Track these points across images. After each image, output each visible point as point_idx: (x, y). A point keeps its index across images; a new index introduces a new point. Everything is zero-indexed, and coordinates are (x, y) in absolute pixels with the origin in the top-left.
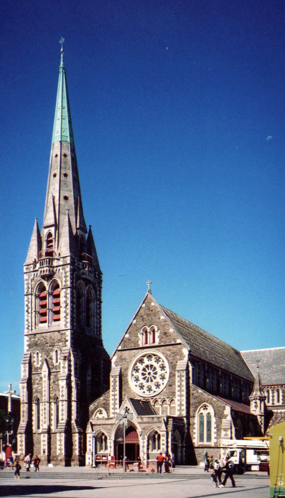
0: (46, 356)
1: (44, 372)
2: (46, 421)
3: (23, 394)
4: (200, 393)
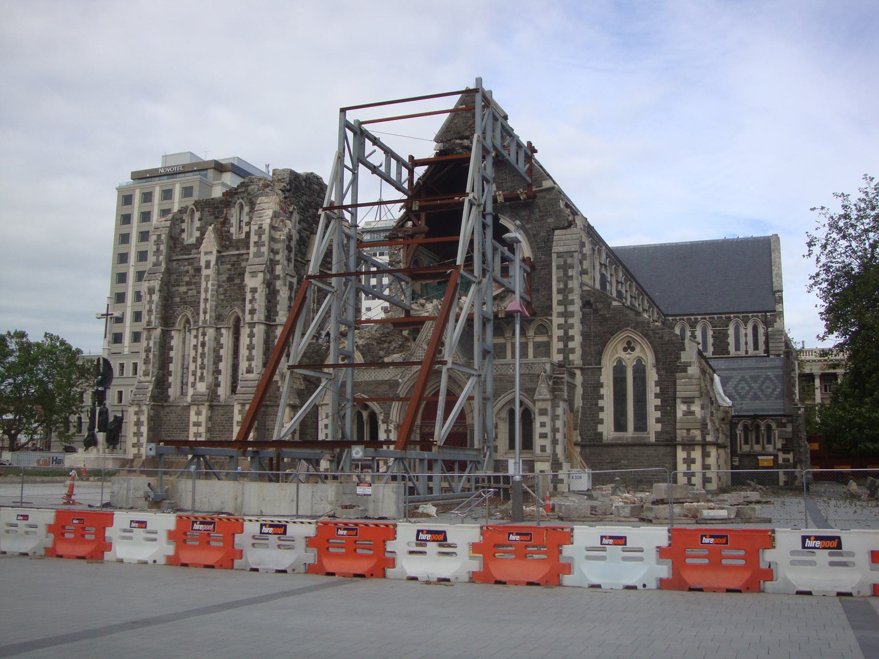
0: (213, 217)
1: (206, 253)
2: (205, 374)
3: (151, 307)
4: (616, 307)
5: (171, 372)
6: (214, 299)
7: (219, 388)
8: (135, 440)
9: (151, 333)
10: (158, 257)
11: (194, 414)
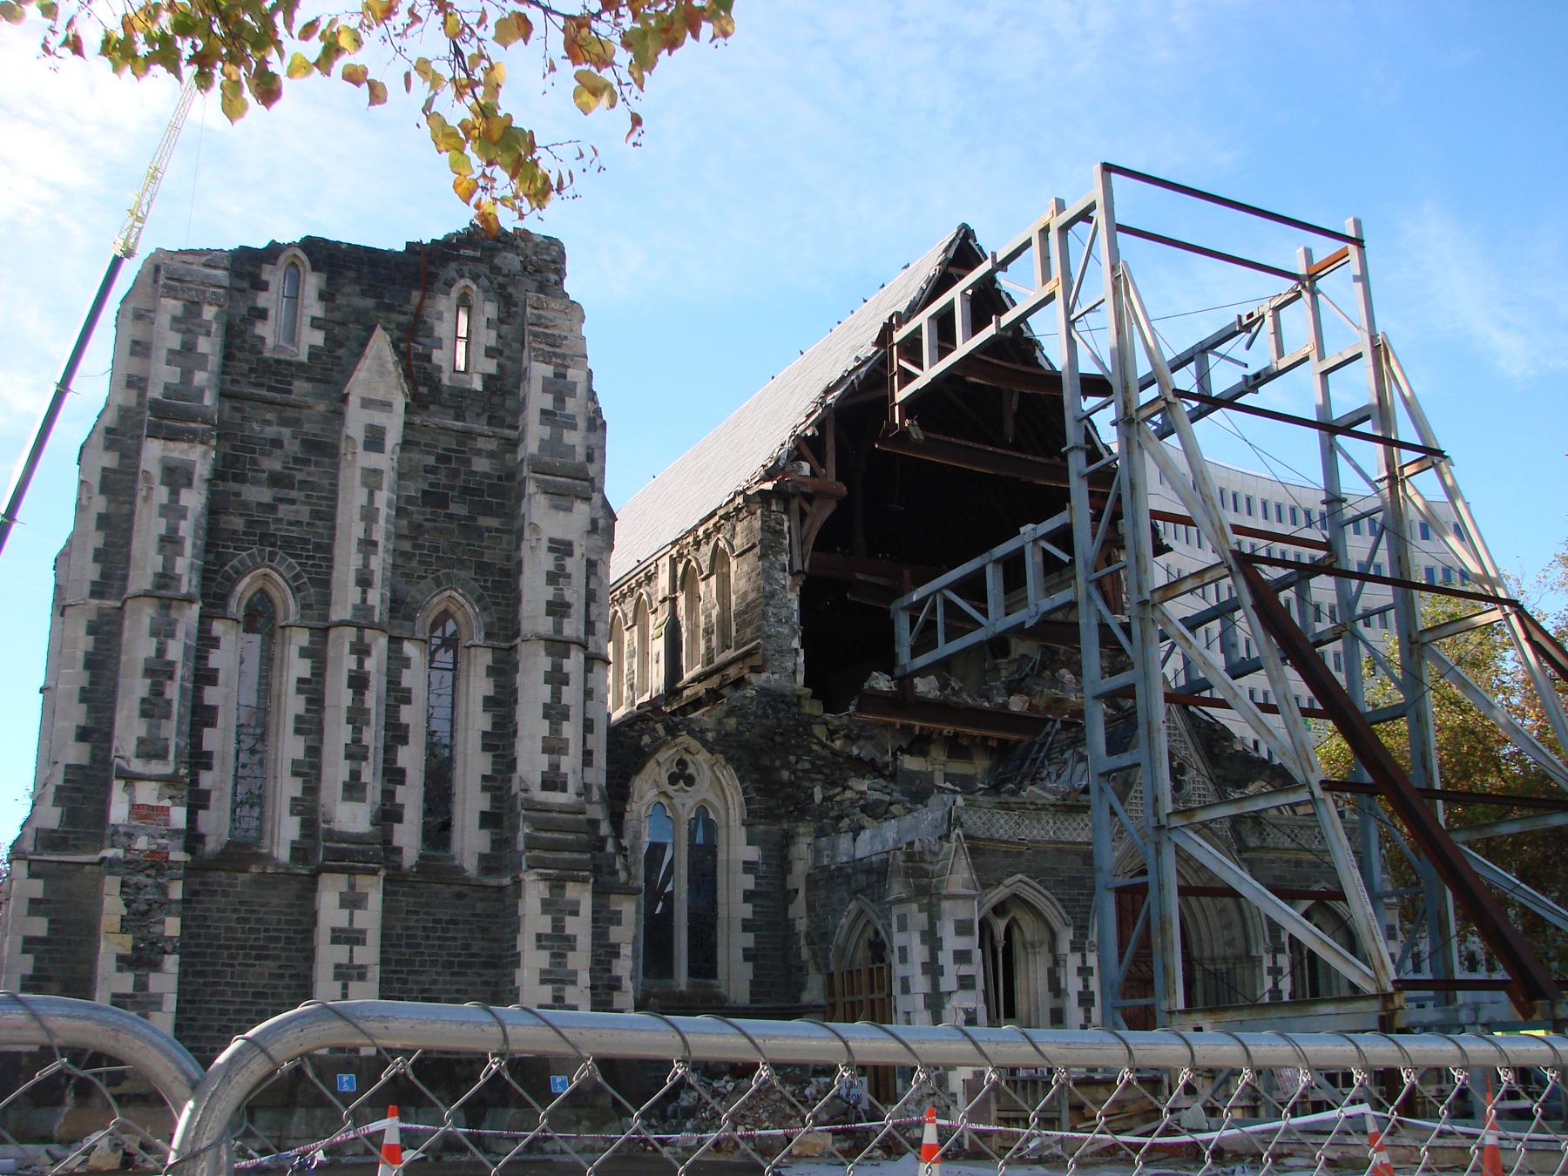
1: (367, 403)
2: (366, 777)
5: (209, 754)
6: (391, 547)
7: (396, 826)
8: (125, 983)
9: (174, 614)
10: (187, 375)
11: (336, 900)
